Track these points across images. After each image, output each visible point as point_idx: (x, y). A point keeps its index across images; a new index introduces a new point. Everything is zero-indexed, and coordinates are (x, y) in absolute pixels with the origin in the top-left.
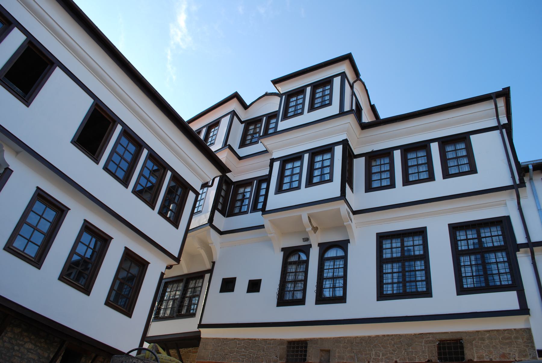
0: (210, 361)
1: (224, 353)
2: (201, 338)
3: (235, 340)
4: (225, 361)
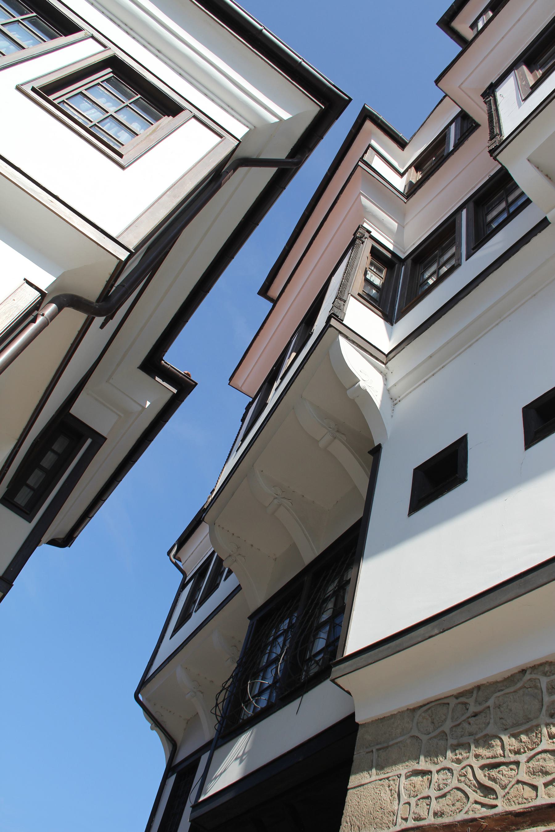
0: (411, 823)
1: (476, 764)
2: (357, 725)
3: (528, 676)
4: (495, 806)
